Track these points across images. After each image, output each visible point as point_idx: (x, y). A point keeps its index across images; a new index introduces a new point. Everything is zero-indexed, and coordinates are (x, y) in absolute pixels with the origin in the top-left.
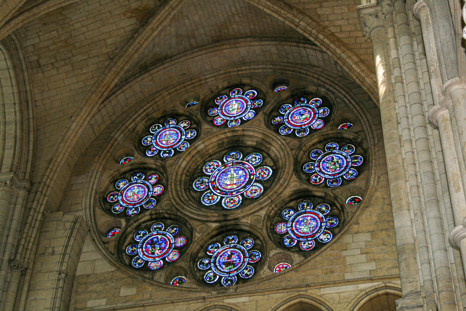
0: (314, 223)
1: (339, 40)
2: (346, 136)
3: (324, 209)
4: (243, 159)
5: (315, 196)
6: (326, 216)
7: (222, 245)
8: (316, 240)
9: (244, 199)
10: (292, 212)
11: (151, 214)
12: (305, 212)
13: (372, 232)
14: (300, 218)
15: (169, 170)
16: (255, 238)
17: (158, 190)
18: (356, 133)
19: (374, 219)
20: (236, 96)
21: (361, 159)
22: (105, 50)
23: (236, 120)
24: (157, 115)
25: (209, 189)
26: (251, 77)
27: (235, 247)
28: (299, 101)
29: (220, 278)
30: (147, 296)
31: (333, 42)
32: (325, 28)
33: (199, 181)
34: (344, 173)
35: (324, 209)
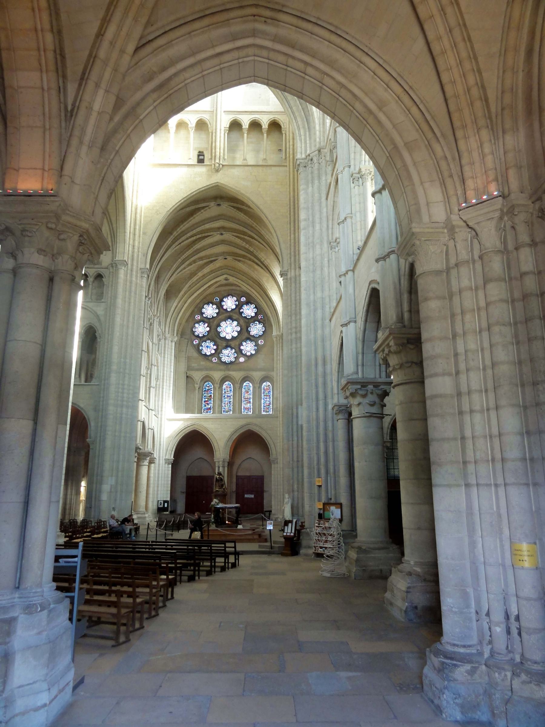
0: (250, 347)
14: (247, 345)
15: (211, 323)
17: (208, 329)
24: (206, 302)
26: (235, 293)
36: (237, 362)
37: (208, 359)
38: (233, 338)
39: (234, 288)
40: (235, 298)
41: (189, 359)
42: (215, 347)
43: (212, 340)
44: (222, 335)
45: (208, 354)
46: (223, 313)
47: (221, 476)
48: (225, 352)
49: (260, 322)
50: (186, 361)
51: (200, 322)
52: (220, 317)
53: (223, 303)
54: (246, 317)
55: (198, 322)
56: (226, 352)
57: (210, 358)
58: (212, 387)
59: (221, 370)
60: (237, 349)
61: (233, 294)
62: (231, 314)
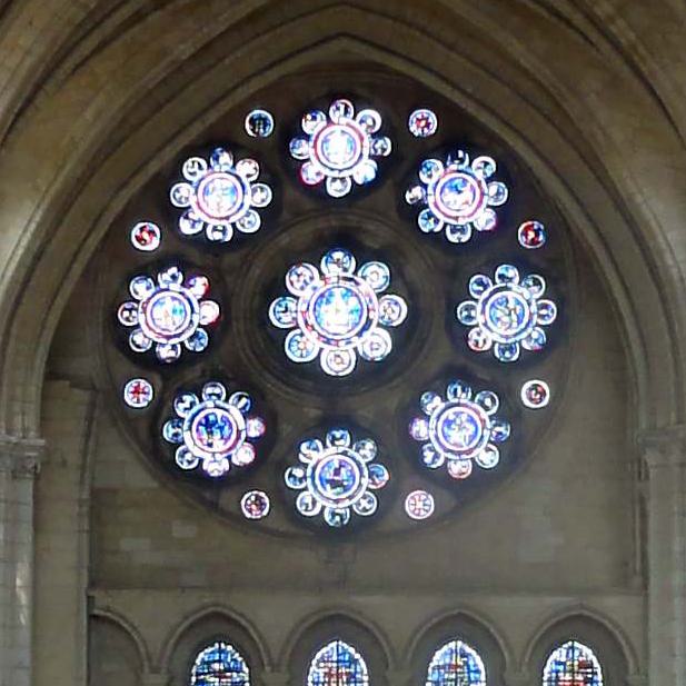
0: (472, 428)
2: (534, 259)
3: (488, 402)
4: (355, 273)
6: (491, 418)
7: (325, 446)
8: (473, 460)
9: (360, 360)
10: (437, 400)
11: (203, 371)
12: (458, 405)
14: (450, 414)
17: (211, 312)
20: (344, 120)
21: (553, 311)
23: (343, 180)
25: (297, 327)
27: (345, 453)
29: (323, 508)
33: (280, 306)
34: (524, 335)
35: (488, 402)
37: (213, 506)
38: (367, 370)
40: (373, 116)
41: (100, 506)
42: (255, 428)
43: (235, 382)
45: (216, 467)
48: (314, 454)
49: (526, 268)
51: (163, 269)
52: (284, 240)
53: (301, 149)
54: (438, 238)
55: (150, 267)
56: (318, 456)
57: (225, 498)
61: (360, 91)
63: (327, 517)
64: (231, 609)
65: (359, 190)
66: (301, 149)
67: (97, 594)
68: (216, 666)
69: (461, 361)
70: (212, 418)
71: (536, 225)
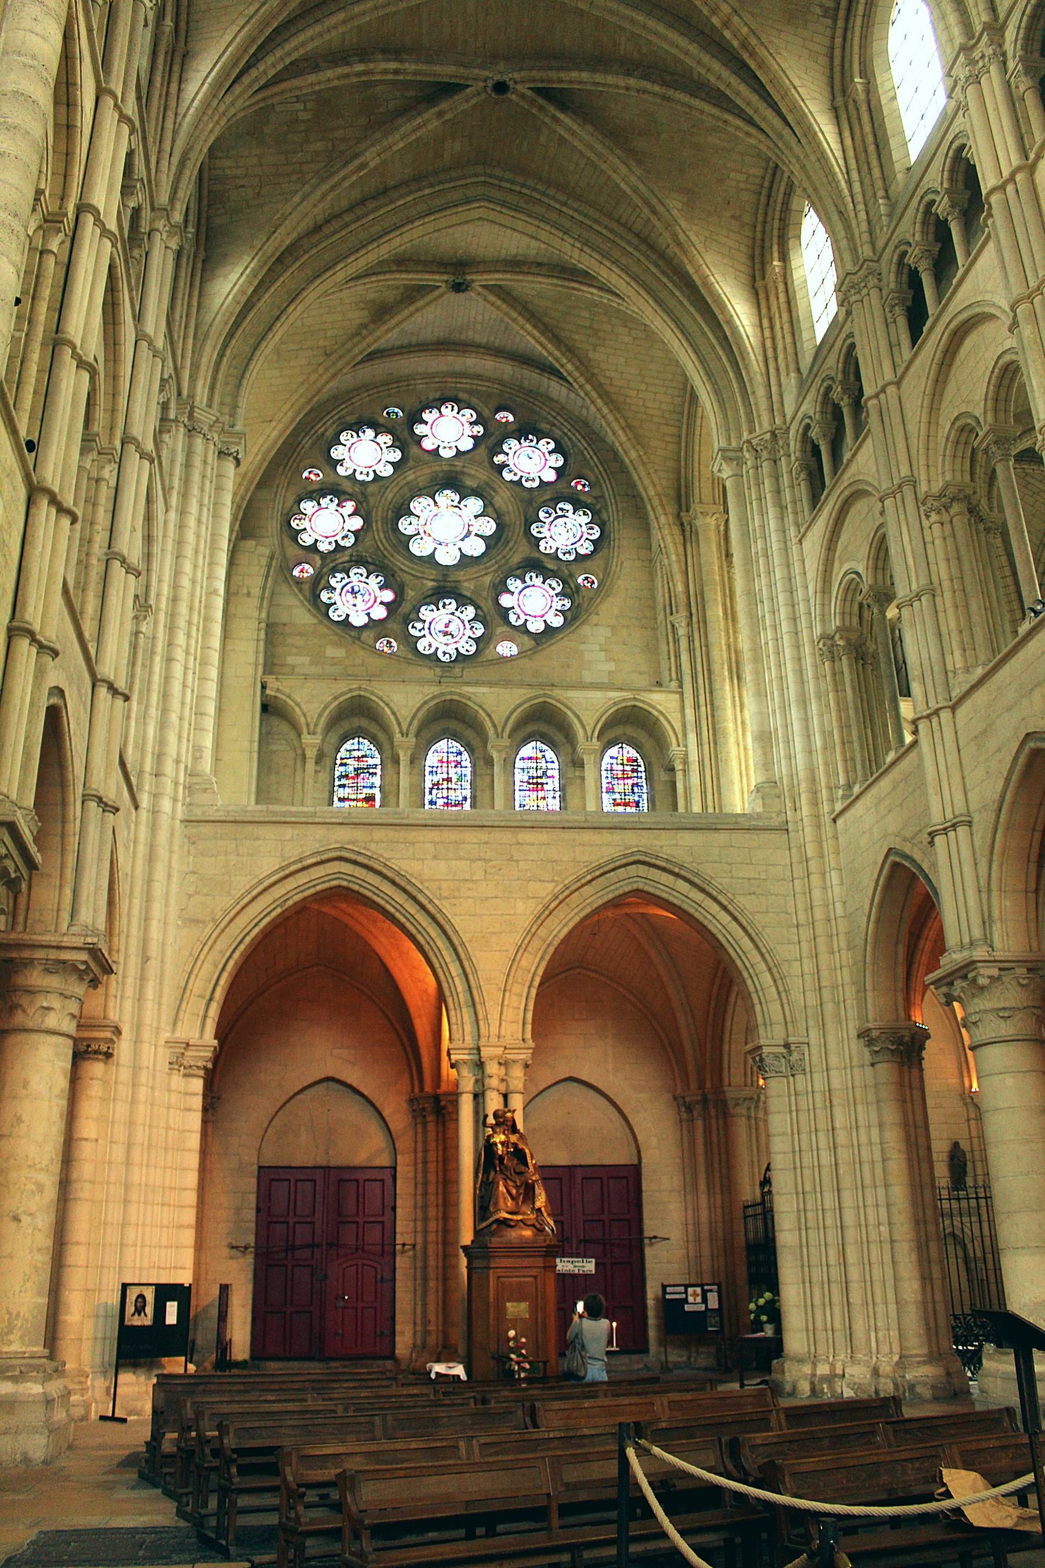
1: (607, 393)
2: (583, 498)
3: (554, 584)
5: (545, 568)
6: (557, 595)
9: (463, 555)
10: (519, 582)
13: (613, 627)
15: (372, 500)
16: (477, 607)
17: (357, 523)
18: (596, 498)
19: (616, 612)
22: (321, 343)
24: (351, 419)
26: (471, 392)
28: (526, 439)
30: (358, 661)
31: (600, 396)
32: (593, 375)
36: (488, 655)
38: (465, 561)
39: (471, 363)
42: (388, 596)
43: (374, 564)
44: (417, 548)
45: (358, 620)
46: (419, 463)
47: (514, 1138)
49: (578, 505)
50: (262, 635)
51: (324, 497)
52: (410, 476)
53: (420, 429)
54: (519, 483)
55: (316, 494)
57: (366, 635)
58: (377, 761)
59: (422, 682)
60: (487, 605)
61: (463, 396)
62: (459, 463)
63: (440, 654)
64: (372, 693)
65: (459, 453)
66: (420, 429)
67: (270, 680)
68: (356, 754)
69: (537, 555)
70: (356, 589)
71: (583, 482)
